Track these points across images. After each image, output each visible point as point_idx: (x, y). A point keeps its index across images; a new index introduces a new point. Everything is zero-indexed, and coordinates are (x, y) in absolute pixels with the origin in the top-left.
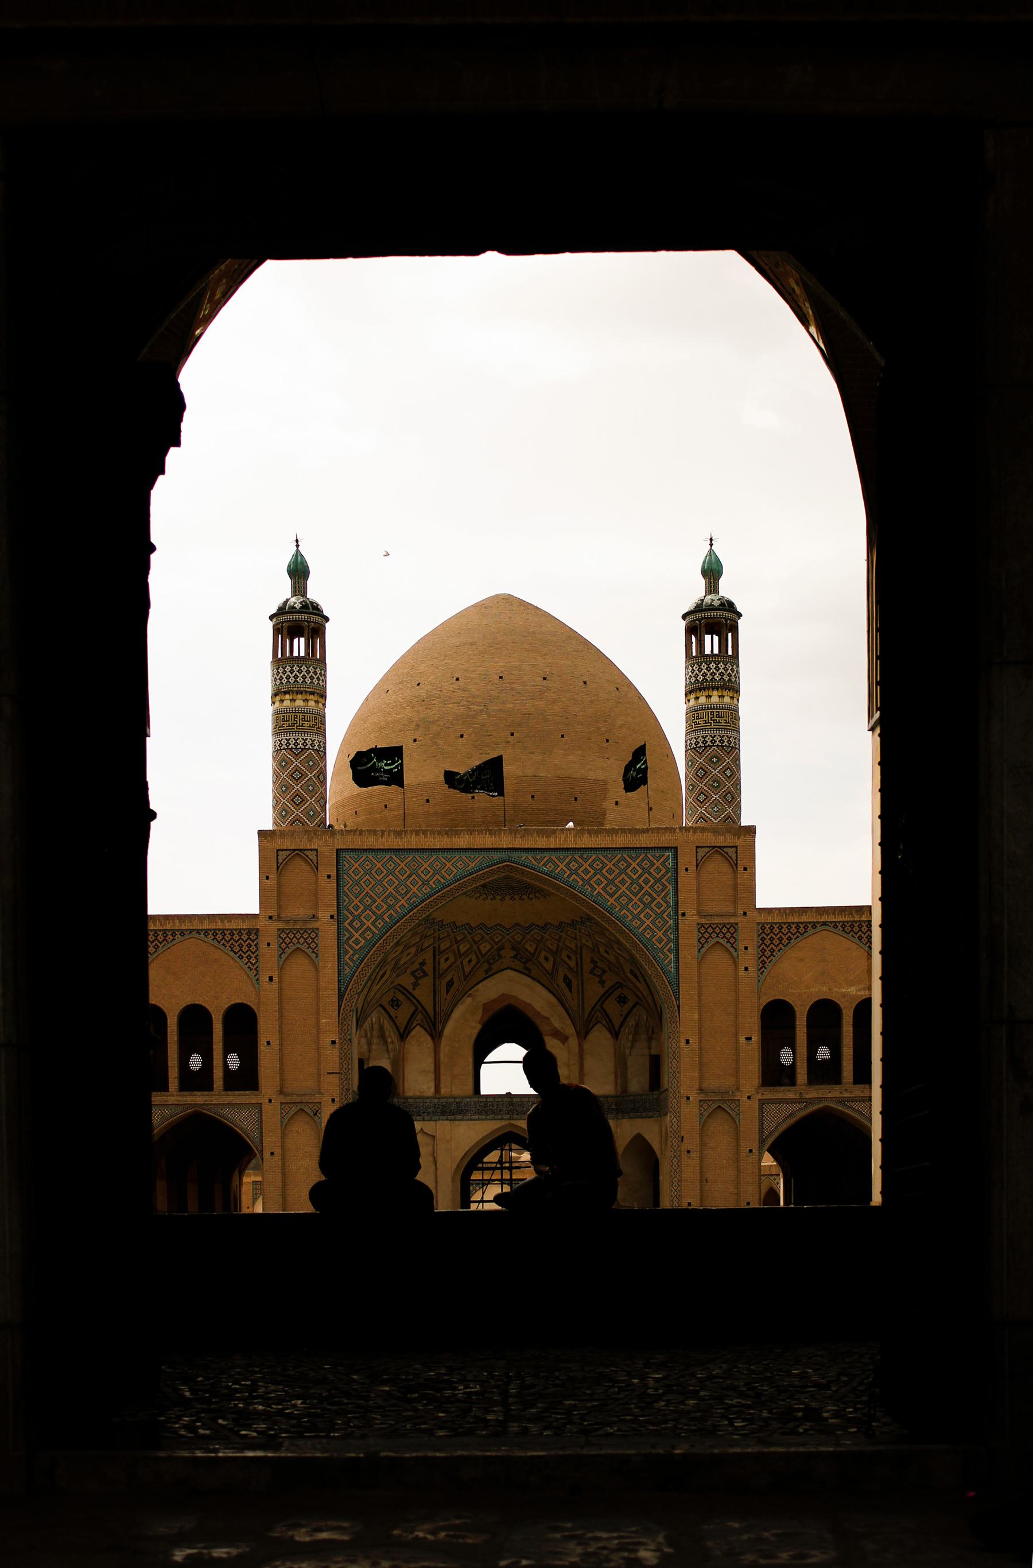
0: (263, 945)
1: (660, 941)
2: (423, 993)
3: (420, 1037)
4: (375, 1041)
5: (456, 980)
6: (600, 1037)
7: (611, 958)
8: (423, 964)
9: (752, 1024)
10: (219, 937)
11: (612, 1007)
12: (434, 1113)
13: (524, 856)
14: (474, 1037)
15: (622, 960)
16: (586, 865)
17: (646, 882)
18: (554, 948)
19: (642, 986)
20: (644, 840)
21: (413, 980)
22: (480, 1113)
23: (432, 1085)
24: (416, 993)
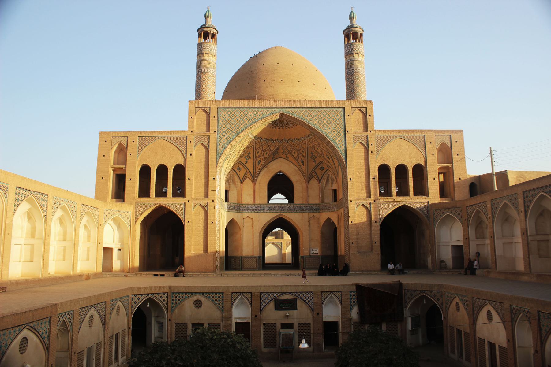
0: (188, 142)
1: (339, 141)
2: (250, 165)
3: (248, 182)
4: (231, 183)
5: (261, 160)
6: (314, 183)
7: (319, 151)
8: (249, 154)
9: (374, 172)
10: (172, 139)
11: (318, 171)
12: (253, 210)
13: (287, 109)
14: (268, 180)
15: (323, 151)
16: (311, 113)
17: (333, 120)
18: (298, 148)
19: (331, 161)
20: (332, 105)
21: (245, 160)
22: (270, 210)
23: (252, 199)
24: (246, 165)
